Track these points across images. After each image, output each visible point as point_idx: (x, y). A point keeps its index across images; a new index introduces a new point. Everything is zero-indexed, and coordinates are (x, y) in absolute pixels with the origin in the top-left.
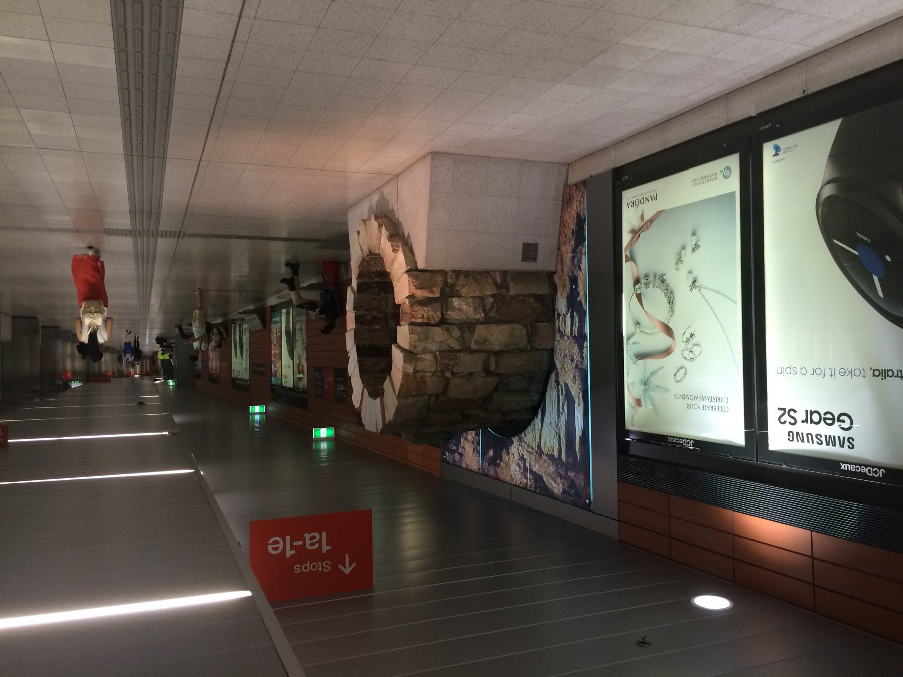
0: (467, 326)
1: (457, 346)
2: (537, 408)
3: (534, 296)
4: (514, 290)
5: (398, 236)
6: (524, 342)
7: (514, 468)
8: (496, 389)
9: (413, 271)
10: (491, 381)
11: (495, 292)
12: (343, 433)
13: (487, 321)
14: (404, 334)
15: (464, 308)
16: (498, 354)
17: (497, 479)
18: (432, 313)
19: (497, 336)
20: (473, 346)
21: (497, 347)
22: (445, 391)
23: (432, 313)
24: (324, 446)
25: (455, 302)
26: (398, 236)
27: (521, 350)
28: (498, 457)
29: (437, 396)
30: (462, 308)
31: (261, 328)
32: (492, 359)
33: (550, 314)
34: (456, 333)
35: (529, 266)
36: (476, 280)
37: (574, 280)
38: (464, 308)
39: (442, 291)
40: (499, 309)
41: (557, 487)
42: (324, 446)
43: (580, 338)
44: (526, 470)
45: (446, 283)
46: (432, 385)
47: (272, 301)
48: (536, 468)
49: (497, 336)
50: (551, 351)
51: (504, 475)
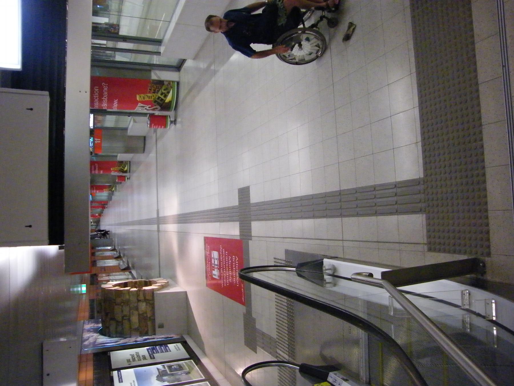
0: (137, 309)
1: (131, 306)
2: (110, 336)
3: (148, 330)
4: (149, 323)
5: (163, 287)
6: (133, 327)
7: (89, 335)
8: (117, 322)
9: (153, 291)
10: (119, 319)
11: (149, 316)
12: (84, 296)
13: (139, 315)
14: (135, 289)
15: (143, 307)
16: (129, 320)
17: (83, 333)
18: (141, 297)
19: (135, 319)
20: (131, 311)
21: (131, 319)
22: (116, 305)
23: (141, 297)
24: (79, 289)
25: (144, 304)
26: (163, 287)
27: (131, 328)
28: (91, 332)
29: (115, 302)
30: (143, 306)
31: (122, 268)
32: (128, 318)
33: (141, 335)
34: (136, 305)
35: (157, 326)
36: (151, 311)
37: (154, 338)
38: (143, 307)
39: (148, 300)
40: (143, 318)
41: (86, 343)
42: (79, 289)
43: (136, 341)
44: (89, 338)
45: (150, 300)
46: (119, 300)
47: (134, 272)
48: (90, 339)
49: (135, 319)
50: (130, 337)
51: (84, 334)
